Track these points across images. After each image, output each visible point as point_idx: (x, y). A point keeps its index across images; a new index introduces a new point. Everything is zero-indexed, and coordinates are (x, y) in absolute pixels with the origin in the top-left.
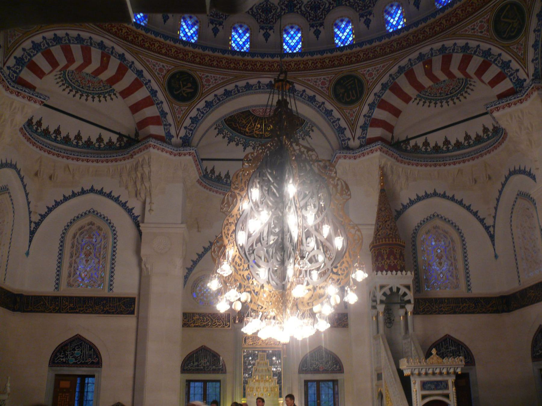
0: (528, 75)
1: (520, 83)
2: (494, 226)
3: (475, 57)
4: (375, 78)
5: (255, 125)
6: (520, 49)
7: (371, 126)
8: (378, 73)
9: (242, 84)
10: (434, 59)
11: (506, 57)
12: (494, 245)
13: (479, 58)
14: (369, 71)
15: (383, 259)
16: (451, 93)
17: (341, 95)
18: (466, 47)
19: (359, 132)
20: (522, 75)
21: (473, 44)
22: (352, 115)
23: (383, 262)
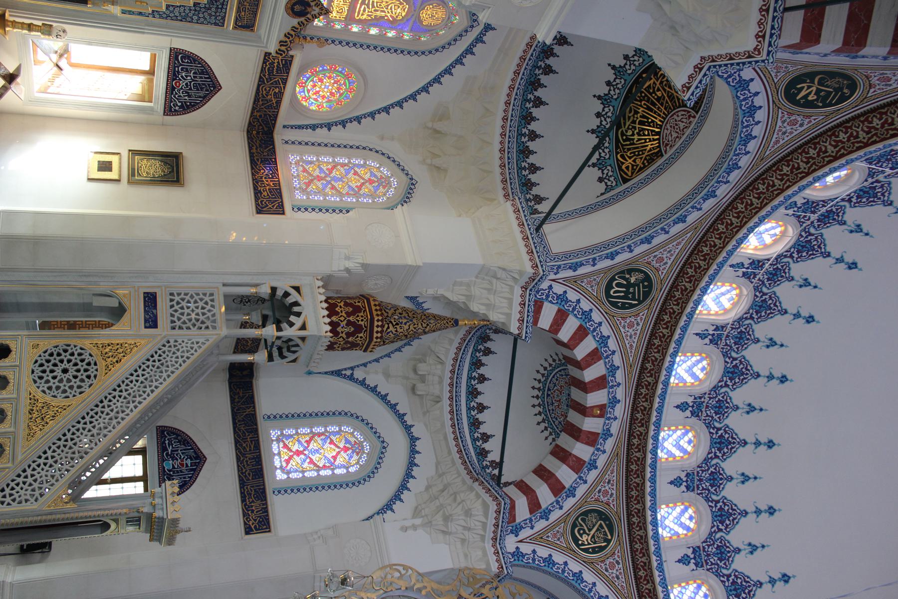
0: (521, 541)
1: (516, 531)
2: (351, 378)
3: (576, 476)
4: (622, 330)
5: (665, 90)
6: (555, 535)
7: (559, 310)
8: (627, 336)
9: (744, 162)
10: (601, 421)
11: (555, 515)
12: (326, 373)
13: (570, 483)
14: (638, 324)
15: (349, 335)
16: (548, 395)
17: (627, 276)
18: (593, 465)
19: (558, 289)
20: (525, 533)
21: (592, 476)
22: (589, 283)
23: (345, 336)
